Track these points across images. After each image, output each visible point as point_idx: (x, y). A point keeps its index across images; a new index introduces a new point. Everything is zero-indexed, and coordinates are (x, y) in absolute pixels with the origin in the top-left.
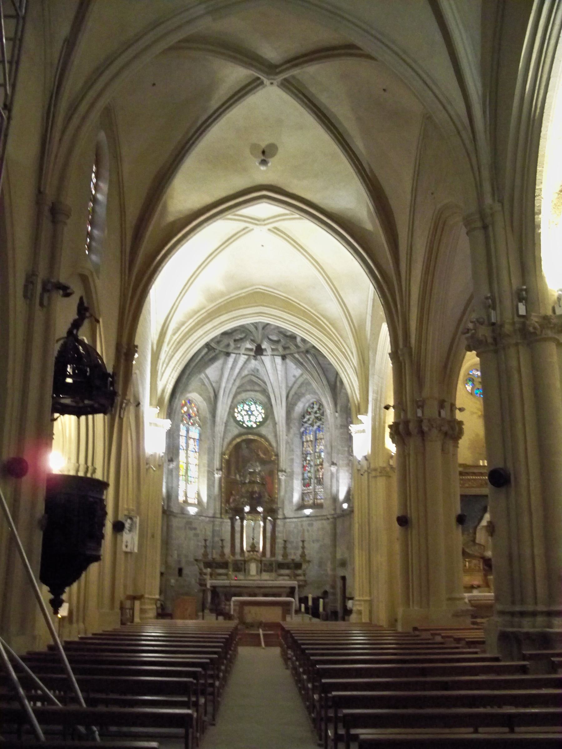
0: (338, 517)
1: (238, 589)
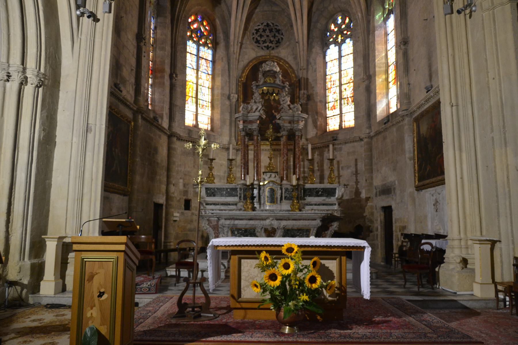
0: (378, 133)
1: (252, 222)
